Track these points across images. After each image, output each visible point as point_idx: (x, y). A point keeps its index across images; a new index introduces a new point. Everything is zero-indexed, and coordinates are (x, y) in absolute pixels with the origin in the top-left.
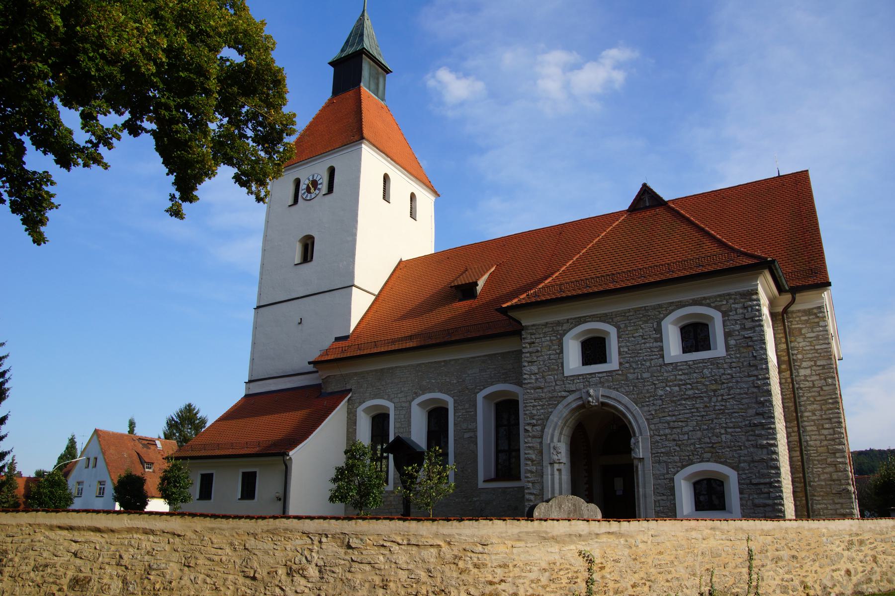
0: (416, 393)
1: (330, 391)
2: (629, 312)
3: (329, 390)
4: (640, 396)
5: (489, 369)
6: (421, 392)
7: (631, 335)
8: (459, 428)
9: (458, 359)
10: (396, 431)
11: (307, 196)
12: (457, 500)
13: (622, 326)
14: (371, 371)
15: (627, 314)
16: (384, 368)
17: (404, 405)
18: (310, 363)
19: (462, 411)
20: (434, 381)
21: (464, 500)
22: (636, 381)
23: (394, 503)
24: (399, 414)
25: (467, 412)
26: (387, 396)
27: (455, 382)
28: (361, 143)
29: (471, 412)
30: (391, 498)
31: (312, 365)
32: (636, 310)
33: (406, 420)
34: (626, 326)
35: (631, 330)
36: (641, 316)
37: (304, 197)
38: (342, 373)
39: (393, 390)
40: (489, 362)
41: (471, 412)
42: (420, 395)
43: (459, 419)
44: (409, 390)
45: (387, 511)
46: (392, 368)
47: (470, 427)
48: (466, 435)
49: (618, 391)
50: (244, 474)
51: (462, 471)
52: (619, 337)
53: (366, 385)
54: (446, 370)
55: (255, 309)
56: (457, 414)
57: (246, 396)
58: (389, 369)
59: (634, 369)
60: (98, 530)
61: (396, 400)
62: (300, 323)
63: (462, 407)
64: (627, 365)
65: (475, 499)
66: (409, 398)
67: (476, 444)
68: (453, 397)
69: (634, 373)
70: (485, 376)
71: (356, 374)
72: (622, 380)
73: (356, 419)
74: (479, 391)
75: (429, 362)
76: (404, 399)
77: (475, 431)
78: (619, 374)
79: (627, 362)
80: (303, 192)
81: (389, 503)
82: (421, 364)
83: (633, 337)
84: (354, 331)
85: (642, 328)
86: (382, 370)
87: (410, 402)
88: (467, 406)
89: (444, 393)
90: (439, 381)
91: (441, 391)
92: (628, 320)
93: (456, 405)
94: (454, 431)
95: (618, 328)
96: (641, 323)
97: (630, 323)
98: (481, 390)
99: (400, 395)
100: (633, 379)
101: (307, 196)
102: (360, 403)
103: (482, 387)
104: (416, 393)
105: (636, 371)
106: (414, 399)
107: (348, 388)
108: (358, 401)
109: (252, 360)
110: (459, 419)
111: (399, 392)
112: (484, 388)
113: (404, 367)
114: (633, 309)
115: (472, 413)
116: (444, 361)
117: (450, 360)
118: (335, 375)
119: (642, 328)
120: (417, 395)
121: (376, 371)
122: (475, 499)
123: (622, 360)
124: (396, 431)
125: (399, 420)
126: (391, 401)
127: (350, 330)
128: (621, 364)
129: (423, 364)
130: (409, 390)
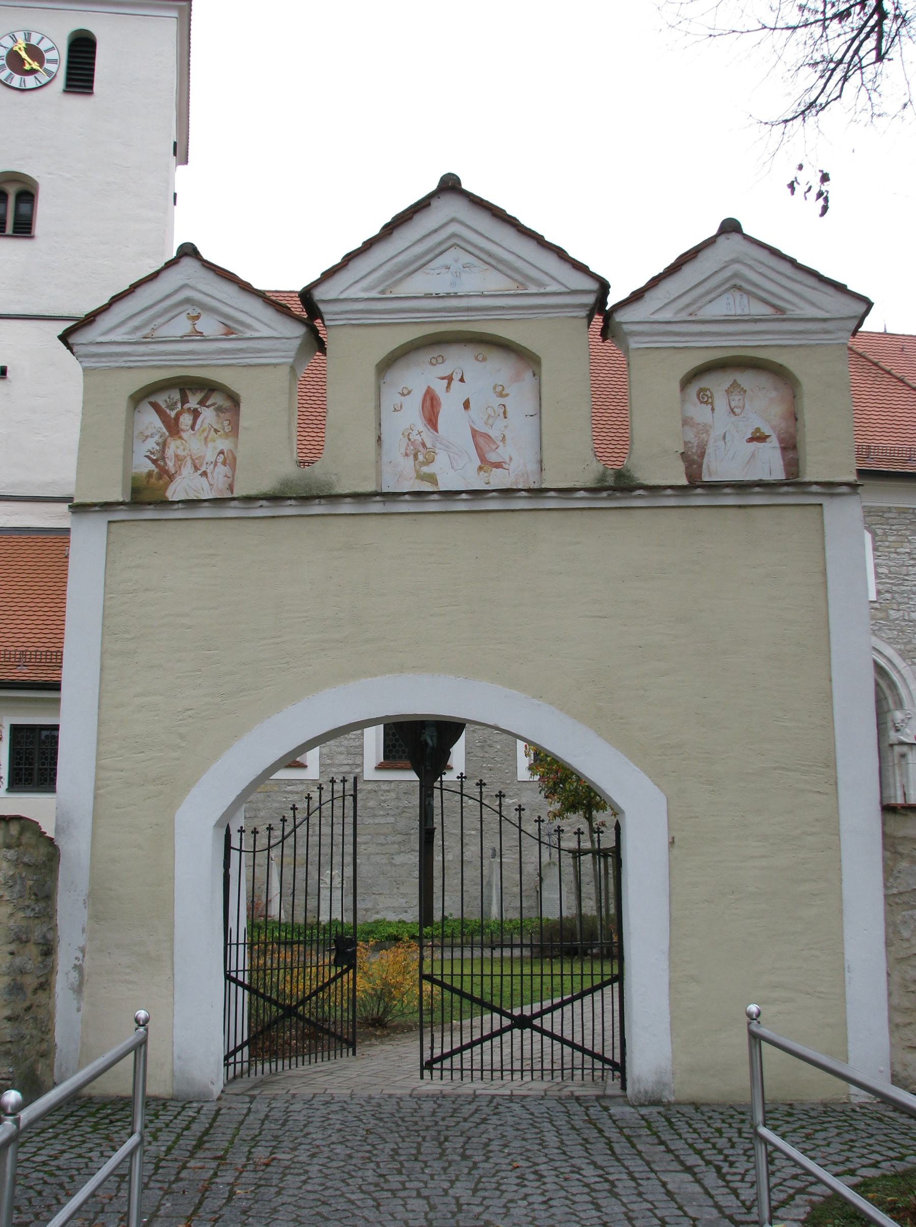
2: (889, 512)
4: (909, 647)
7: (892, 550)
13: (879, 532)
15: (887, 515)
22: (903, 623)
32: (902, 511)
34: (885, 534)
35: (893, 542)
36: (908, 521)
49: (876, 635)
51: (482, 747)
52: (875, 549)
59: (899, 604)
64: (888, 596)
69: (898, 610)
72: (881, 619)
78: (876, 609)
79: (887, 592)
83: (896, 553)
85: (909, 541)
92: (888, 524)
95: (874, 535)
96: (908, 533)
97: (891, 529)
100: (897, 619)
101: (10, 77)
105: (902, 607)
114: (896, 508)
119: (909, 541)
123: (881, 587)
128: (879, 592)
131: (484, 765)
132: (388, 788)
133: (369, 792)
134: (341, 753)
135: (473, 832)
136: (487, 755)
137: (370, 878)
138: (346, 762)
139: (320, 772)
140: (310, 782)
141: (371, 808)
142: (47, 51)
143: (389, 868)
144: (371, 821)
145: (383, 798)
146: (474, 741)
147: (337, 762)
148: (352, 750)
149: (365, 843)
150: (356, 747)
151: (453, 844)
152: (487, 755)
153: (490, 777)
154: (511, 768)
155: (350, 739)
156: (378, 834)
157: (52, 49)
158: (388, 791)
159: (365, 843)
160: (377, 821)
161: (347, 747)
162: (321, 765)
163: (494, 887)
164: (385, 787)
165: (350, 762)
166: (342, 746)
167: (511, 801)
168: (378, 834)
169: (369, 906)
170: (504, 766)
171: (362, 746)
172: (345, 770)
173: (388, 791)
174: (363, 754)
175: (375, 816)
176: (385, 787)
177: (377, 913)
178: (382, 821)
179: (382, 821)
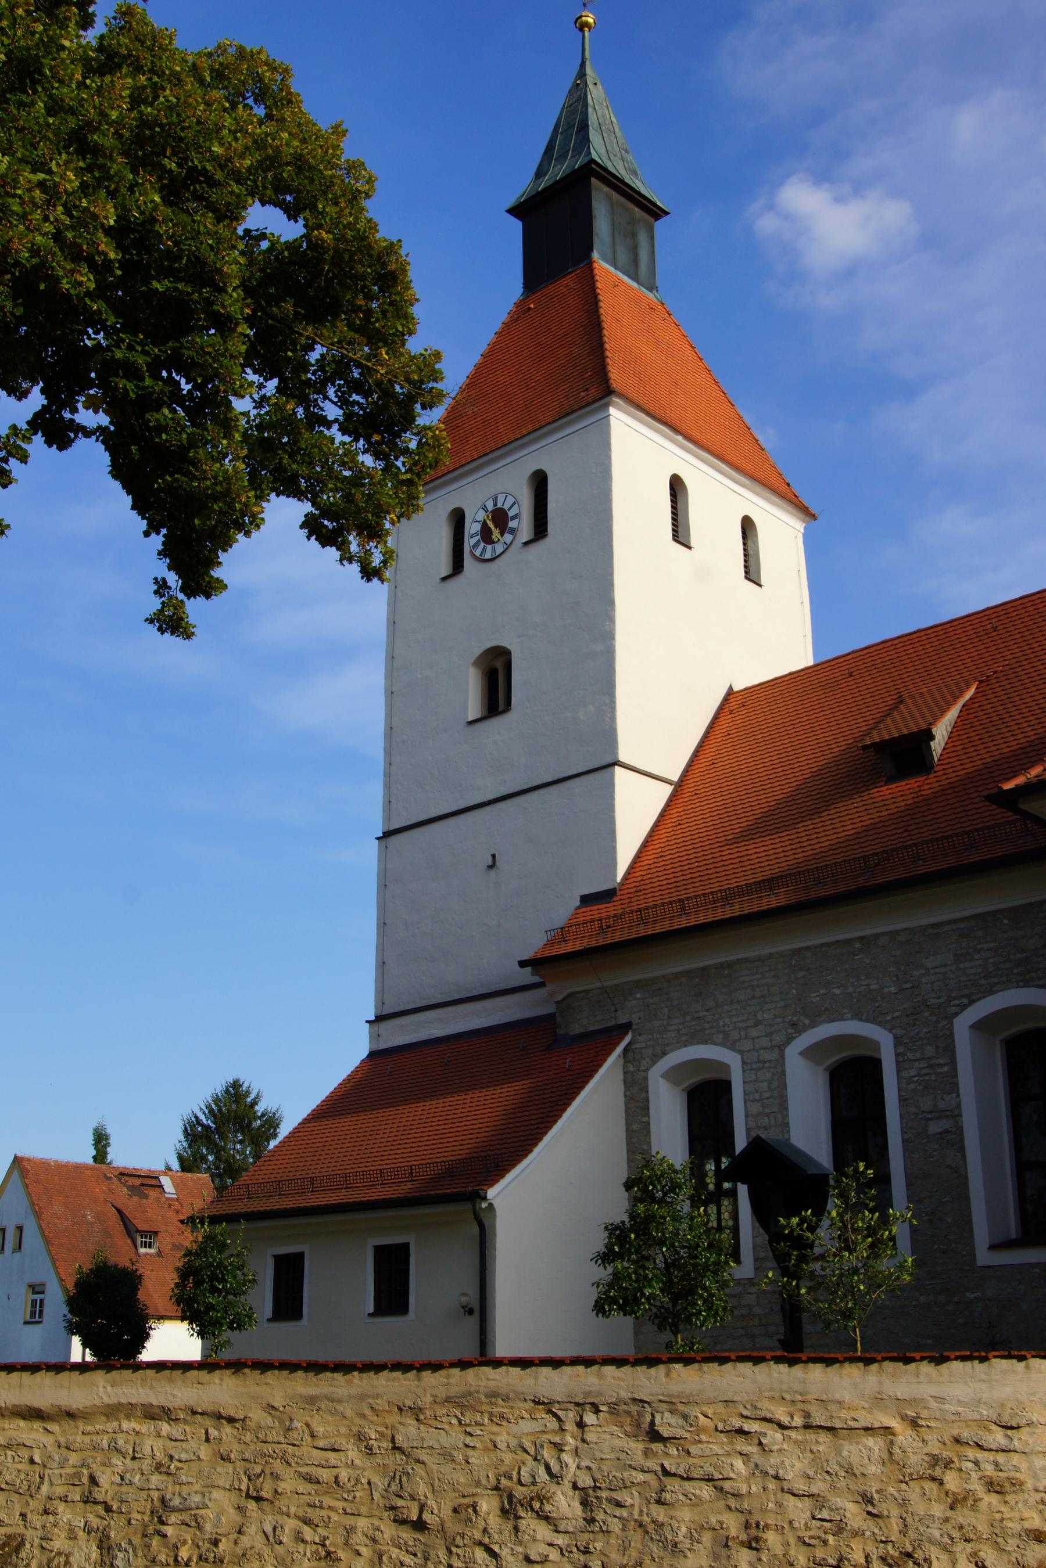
0: (794, 1025)
1: (577, 1031)
3: (576, 1029)
5: (979, 951)
6: (807, 1022)
8: (913, 1110)
9: (898, 932)
10: (752, 1124)
11: (484, 550)
12: (922, 1299)
14: (677, 975)
16: (710, 966)
17: (766, 1055)
18: (522, 964)
19: (917, 1064)
20: (837, 991)
24: (756, 1081)
25: (930, 1067)
26: (721, 1036)
27: (893, 989)
28: (607, 406)
30: (751, 1299)
31: (529, 969)
37: (478, 553)
38: (605, 984)
39: (735, 1019)
40: (980, 933)
42: (805, 1029)
43: (913, 1086)
44: (776, 1017)
46: (729, 965)
47: (941, 1105)
48: (934, 1127)
50: (379, 1250)
53: (666, 1010)
54: (868, 961)
55: (377, 838)
56: (905, 1074)
57: (373, 1055)
58: (722, 966)
60: (34, 1414)
61: (747, 1045)
62: (491, 867)
63: (918, 1055)
65: (970, 1296)
66: (777, 1039)
67: (962, 1149)
68: (890, 1030)
70: (973, 971)
71: (640, 984)
73: (647, 1100)
74: (958, 1009)
75: (823, 945)
76: (765, 1042)
77: (955, 1114)
80: (473, 541)
81: (744, 1311)
82: (801, 949)
84: (626, 877)
86: (704, 969)
87: (781, 1049)
88: (930, 1051)
89: (867, 1021)
90: (851, 990)
91: (858, 1016)
93: (901, 1049)
94: (901, 1116)
98: (963, 1007)
99: (753, 1032)
101: (484, 550)
102: (656, 1058)
103: (965, 1001)
104: (794, 1025)
106: (790, 1040)
107: (622, 1020)
108: (650, 1051)
109: (382, 965)
110: (913, 1086)
111: (751, 1023)
112: (972, 1002)
113: (760, 959)
115: (946, 1069)
116: (861, 939)
117: (877, 936)
118: (587, 992)
120: (797, 1029)
121: (688, 973)
122: (970, 1296)
124: (752, 1124)
125: (757, 1096)
126: (732, 1047)
127: (615, 875)
129: (808, 948)
130: (776, 1017)
135: (929, 1341)
139: (756, 1269)
140: (746, 1282)
142: (509, 509)
157: (514, 503)
167: (972, 1296)
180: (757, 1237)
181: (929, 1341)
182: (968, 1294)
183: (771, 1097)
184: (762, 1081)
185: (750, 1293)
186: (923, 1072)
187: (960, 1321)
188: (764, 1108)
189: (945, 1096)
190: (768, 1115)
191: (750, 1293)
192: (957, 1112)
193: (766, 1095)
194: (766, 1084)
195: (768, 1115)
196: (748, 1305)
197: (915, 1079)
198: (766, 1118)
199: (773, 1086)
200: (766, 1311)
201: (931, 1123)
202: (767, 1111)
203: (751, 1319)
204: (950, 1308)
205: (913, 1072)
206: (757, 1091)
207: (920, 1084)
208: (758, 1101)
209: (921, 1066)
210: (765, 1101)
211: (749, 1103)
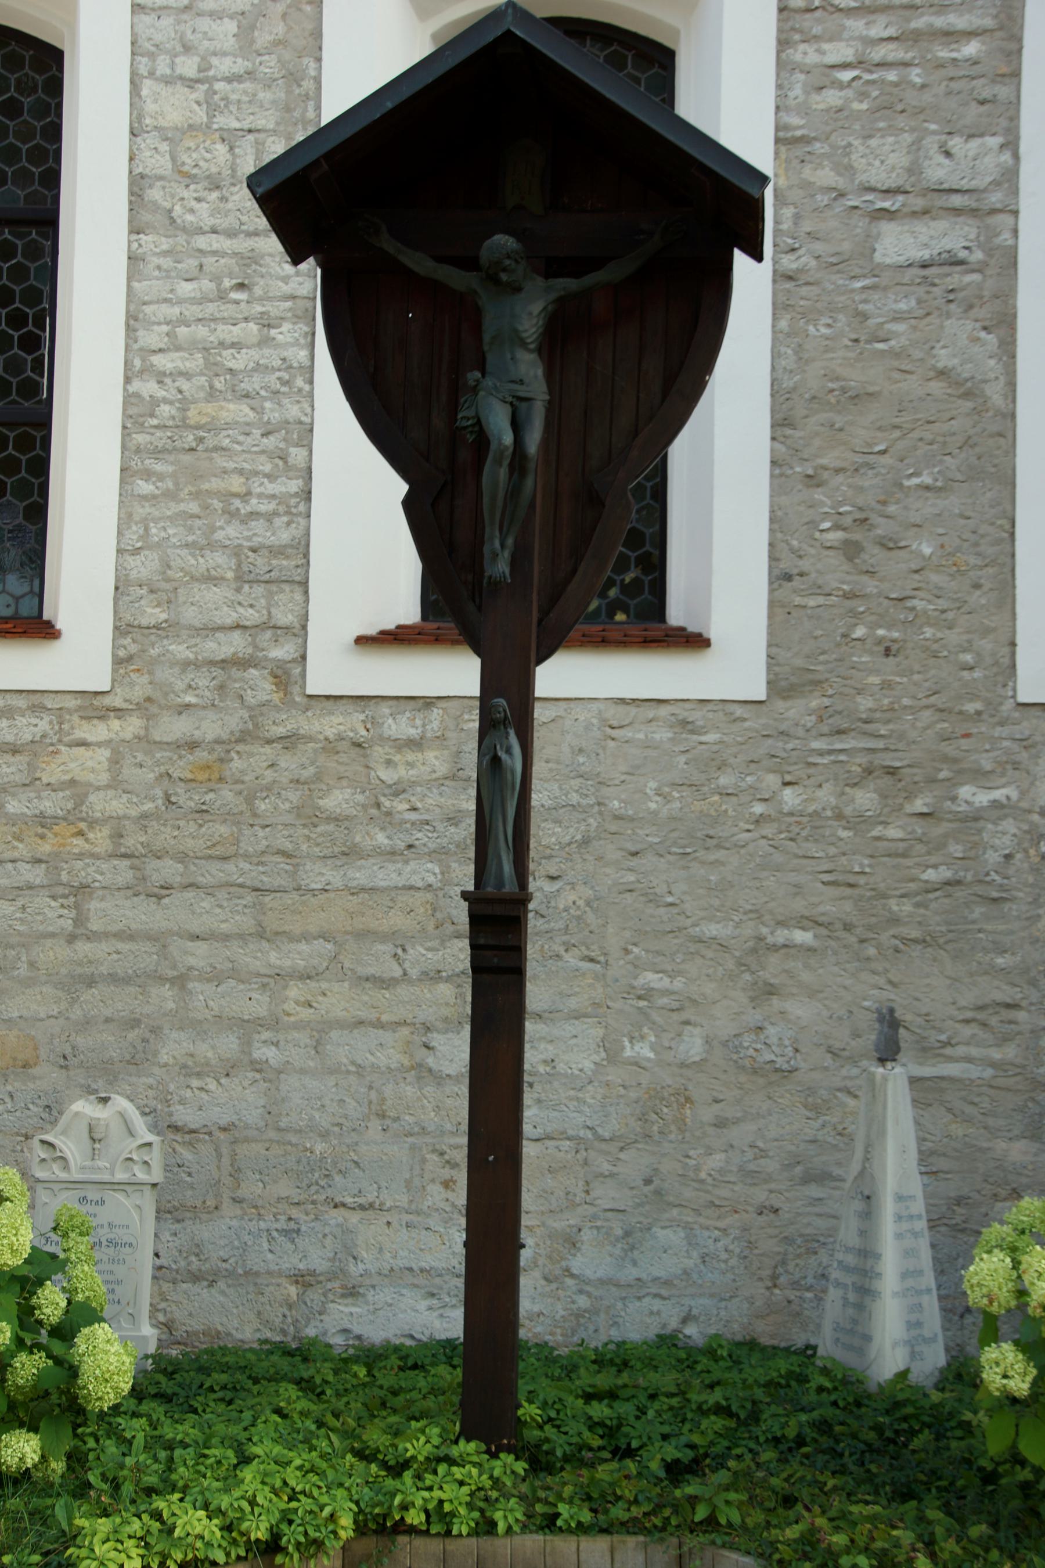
8: (826, 176)
10: (157, 162)
12: (790, 797)
19: (856, 25)
21: (865, 799)
23: (116, 805)
29: (951, 36)
33: (270, 65)
41: (951, 36)
43: (832, 98)
45: (36, 875)
51: (851, 550)
56: (806, 54)
81: (51, 804)
110: (832, 98)
115: (971, 49)
124: (157, 162)
125: (188, 67)
131: (859, 632)
132: (413, 732)
133: (330, 747)
134: (211, 579)
135: (802, 937)
136: (871, 586)
137: (324, 1135)
138: (229, 617)
139: (118, 662)
140: (71, 703)
141: (337, 820)
143: (410, 1091)
144: (333, 876)
145: (388, 775)
146: (812, 524)
147: (190, 615)
148: (261, 563)
149: (306, 977)
150: (277, 551)
151: (709, 988)
152: (871, 586)
153: (887, 685)
154: (986, 645)
155: (254, 515)
156: (364, 935)
158: (415, 744)
159: (306, 977)
160: (360, 875)
161: (237, 552)
162: (121, 630)
163: (888, 1209)
164: (400, 726)
165: (251, 616)
166: (212, 546)
167: (983, 798)
168: (364, 935)
169: (317, 1260)
170: (953, 637)
171: (303, 548)
172: (225, 651)
173: (415, 744)
174: (304, 584)
175: (351, 853)
176: (400, 726)
177: (352, 1293)
178: (388, 875)
179: (388, 875)
180: (136, 551)
181: (802, 937)
182: (965, 792)
183: (250, 74)
184: (216, 15)
185: (83, 744)
186: (879, 53)
187: (930, 875)
188: (213, 110)
189: (956, 143)
190: (229, 138)
191: (83, 744)
192: (995, 198)
193: (224, 66)
194: (230, 26)
195: (229, 138)
196: (73, 782)
197: (846, 76)
198: (221, 149)
199: (263, 38)
200: (148, 806)
201: (888, 229)
202: (222, 121)
203: (81, 833)
204: (893, 832)
205: (839, 52)
206: (187, 49)
207: (863, 96)
208: (191, 83)
209: (877, 31)
210: (219, 86)
211: (147, 88)
